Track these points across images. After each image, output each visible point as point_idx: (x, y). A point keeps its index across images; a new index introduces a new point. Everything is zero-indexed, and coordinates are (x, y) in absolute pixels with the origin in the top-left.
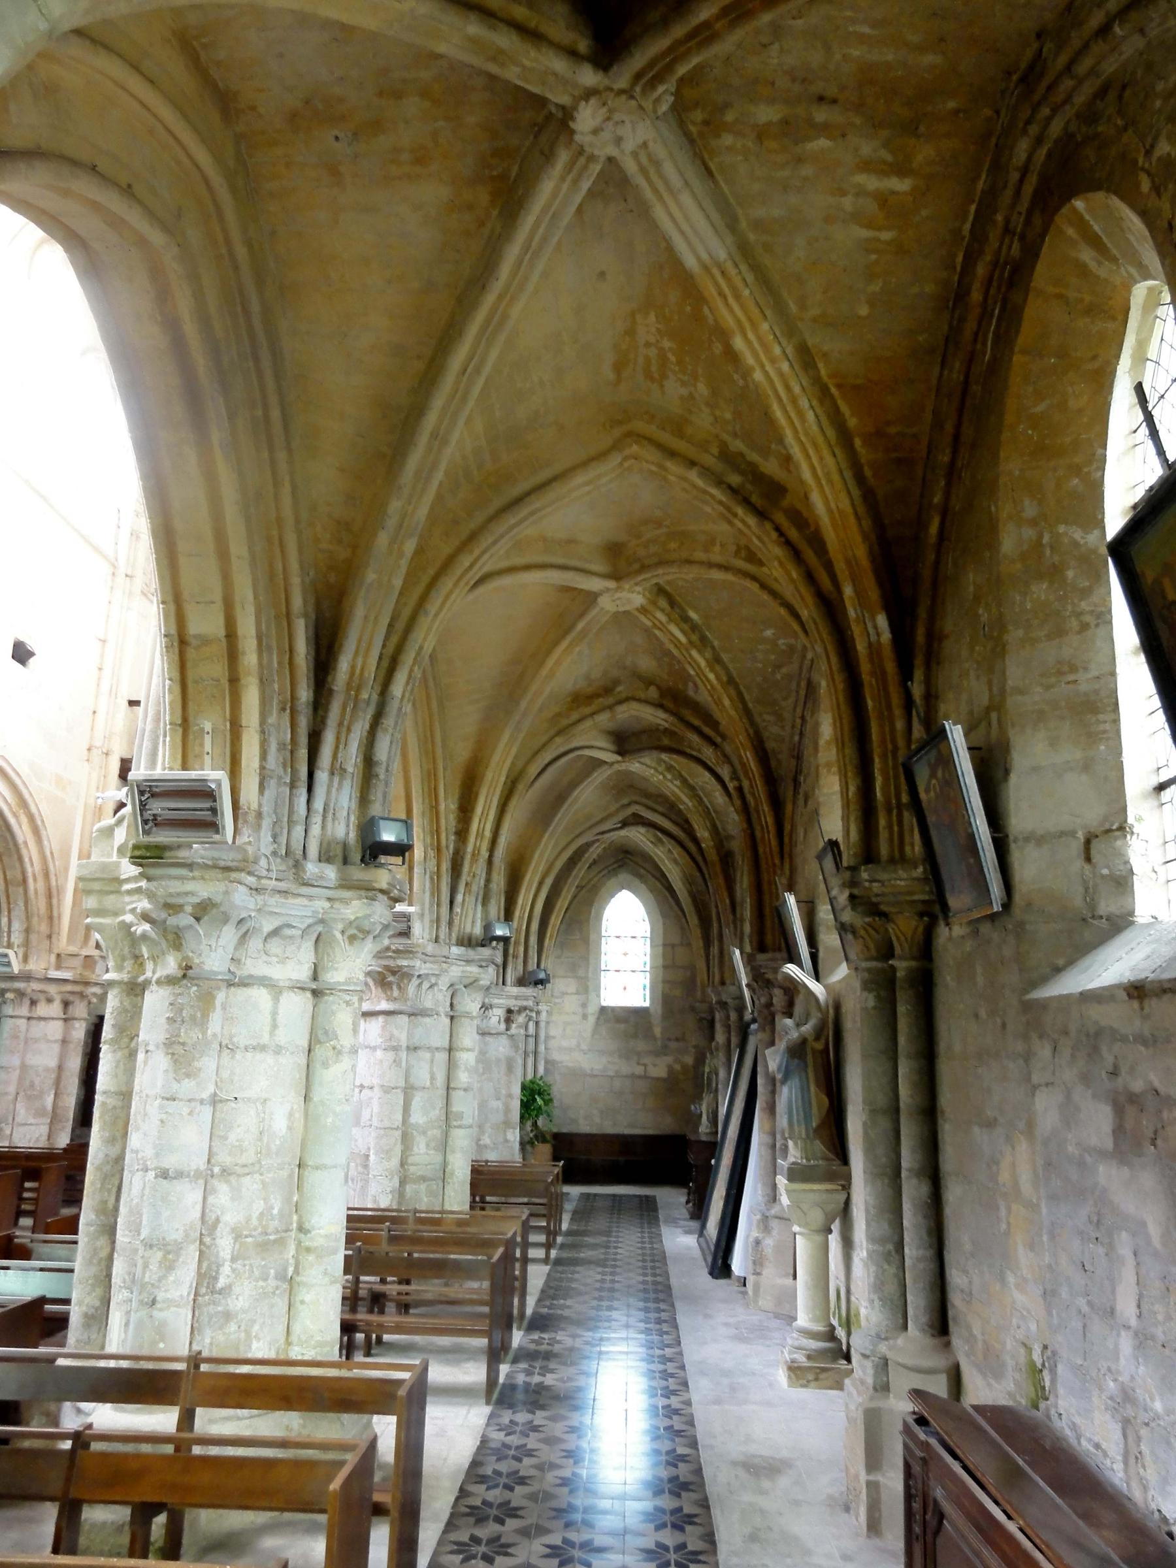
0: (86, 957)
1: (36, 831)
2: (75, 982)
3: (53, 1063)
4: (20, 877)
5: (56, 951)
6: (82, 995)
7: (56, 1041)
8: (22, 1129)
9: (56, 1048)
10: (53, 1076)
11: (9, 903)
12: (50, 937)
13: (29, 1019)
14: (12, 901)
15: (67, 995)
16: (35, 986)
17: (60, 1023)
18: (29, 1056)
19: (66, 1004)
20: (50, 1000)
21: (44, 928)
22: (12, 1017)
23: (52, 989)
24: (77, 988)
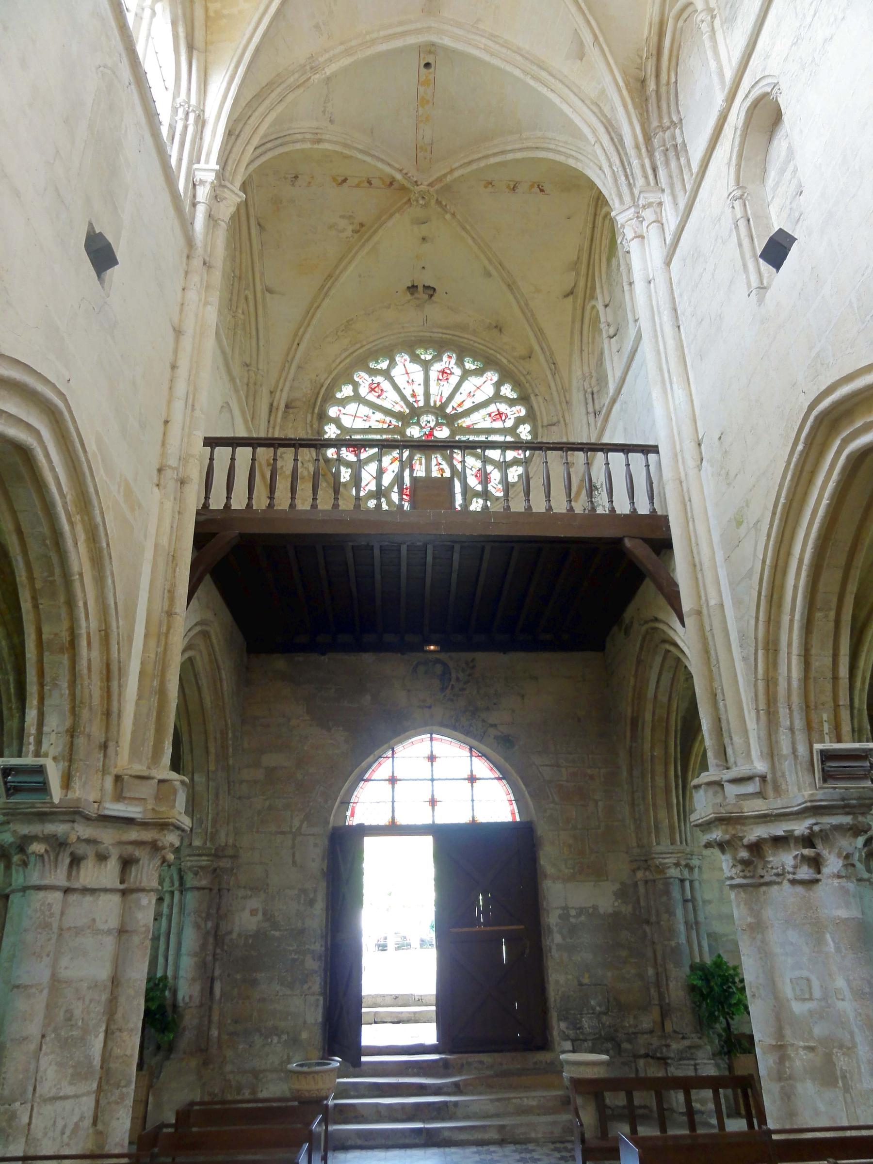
0: (161, 781)
1: (98, 559)
2: (144, 825)
3: (103, 973)
4: (65, 636)
5: (115, 771)
6: (155, 847)
7: (109, 932)
8: (48, 1110)
9: (110, 942)
10: (104, 997)
11: (41, 685)
12: (105, 747)
13: (67, 891)
14: (47, 679)
15: (130, 848)
16: (83, 831)
17: (116, 898)
18: (64, 962)
19: (127, 863)
20: (102, 858)
21: (96, 730)
22: (39, 888)
23: (108, 837)
24: (147, 835)
